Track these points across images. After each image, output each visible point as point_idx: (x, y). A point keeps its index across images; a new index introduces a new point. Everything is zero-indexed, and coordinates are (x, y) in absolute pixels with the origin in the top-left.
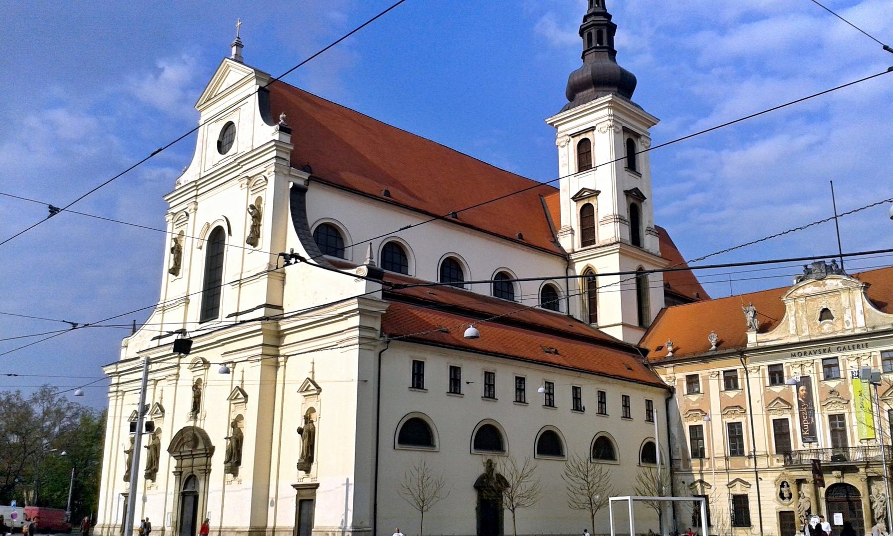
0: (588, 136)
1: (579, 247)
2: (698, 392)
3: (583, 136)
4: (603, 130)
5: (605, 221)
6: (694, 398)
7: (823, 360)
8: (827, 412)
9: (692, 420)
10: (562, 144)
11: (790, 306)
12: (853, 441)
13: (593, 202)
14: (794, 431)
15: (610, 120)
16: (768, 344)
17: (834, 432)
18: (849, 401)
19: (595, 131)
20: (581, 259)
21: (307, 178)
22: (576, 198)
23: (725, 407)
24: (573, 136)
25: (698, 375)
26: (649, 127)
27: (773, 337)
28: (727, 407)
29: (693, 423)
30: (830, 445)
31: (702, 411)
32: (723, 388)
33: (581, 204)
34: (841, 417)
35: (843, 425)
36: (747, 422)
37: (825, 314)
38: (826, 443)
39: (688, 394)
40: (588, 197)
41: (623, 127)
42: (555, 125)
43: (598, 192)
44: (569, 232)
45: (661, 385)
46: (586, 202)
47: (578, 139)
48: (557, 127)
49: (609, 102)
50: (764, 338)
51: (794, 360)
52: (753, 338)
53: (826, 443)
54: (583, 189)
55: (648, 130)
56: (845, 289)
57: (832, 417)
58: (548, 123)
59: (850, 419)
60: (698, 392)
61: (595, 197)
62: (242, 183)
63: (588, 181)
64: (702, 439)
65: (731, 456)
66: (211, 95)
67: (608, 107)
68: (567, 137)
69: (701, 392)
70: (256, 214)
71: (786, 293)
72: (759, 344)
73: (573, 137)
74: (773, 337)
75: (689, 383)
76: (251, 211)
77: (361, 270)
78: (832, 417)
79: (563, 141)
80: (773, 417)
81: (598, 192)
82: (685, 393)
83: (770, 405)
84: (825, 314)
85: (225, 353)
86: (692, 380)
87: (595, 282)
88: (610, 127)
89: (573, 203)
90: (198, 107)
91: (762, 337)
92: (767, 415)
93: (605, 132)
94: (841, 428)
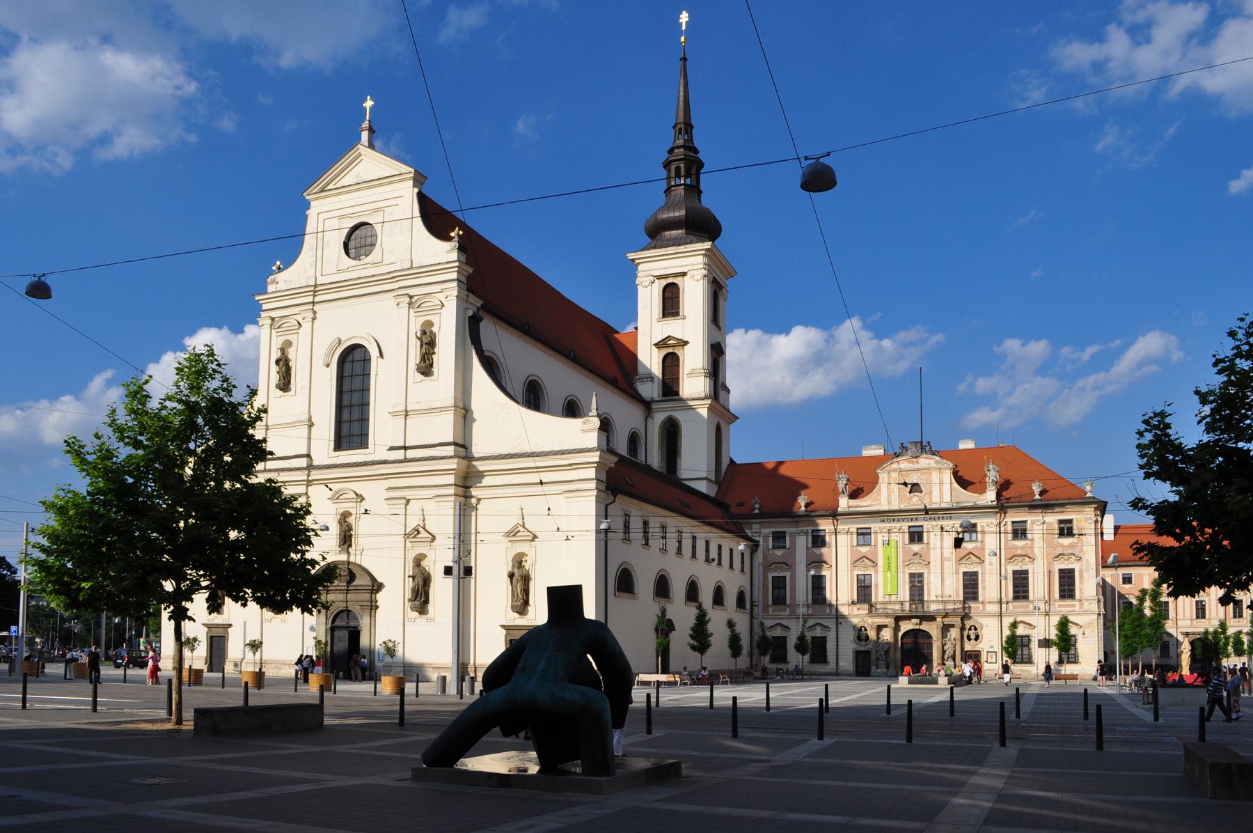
1: (659, 396)
2: (784, 547)
3: (670, 280)
4: (696, 278)
5: (692, 374)
6: (779, 553)
7: (909, 527)
8: (908, 571)
9: (776, 572)
10: (644, 284)
11: (883, 478)
12: (929, 595)
13: (678, 351)
14: (876, 585)
15: (705, 269)
16: (858, 509)
17: (912, 587)
18: (929, 563)
19: (685, 277)
20: (664, 410)
21: (480, 306)
22: (660, 345)
23: (811, 561)
24: (659, 277)
25: (785, 532)
26: (727, 279)
27: (863, 504)
28: (812, 563)
29: (776, 574)
30: (907, 598)
31: (786, 564)
32: (810, 545)
33: (665, 351)
34: (921, 575)
35: (921, 582)
36: (831, 575)
38: (904, 597)
39: (774, 548)
40: (674, 346)
41: (714, 277)
42: (637, 261)
43: (686, 343)
44: (649, 379)
46: (670, 350)
47: (664, 282)
48: (638, 264)
49: (707, 250)
50: (855, 504)
51: (882, 525)
52: (844, 503)
53: (904, 597)
54: (669, 336)
55: (727, 282)
56: (937, 468)
57: (912, 575)
58: (629, 258)
59: (929, 577)
60: (784, 547)
61: (681, 347)
62: (400, 300)
63: (672, 328)
64: (785, 588)
65: (773, 604)
66: (327, 186)
67: (704, 255)
68: (652, 278)
69: (787, 547)
70: (428, 343)
71: (882, 465)
72: (850, 509)
73: (658, 279)
74: (863, 504)
75: (774, 538)
76: (419, 335)
77: (589, 421)
78: (912, 575)
79: (646, 281)
80: (856, 572)
81: (686, 343)
82: (771, 547)
83: (856, 562)
85: (390, 488)
86: (779, 537)
87: (676, 434)
88: (705, 276)
89: (655, 350)
90: (308, 195)
91: (852, 502)
92: (852, 571)
94: (919, 585)
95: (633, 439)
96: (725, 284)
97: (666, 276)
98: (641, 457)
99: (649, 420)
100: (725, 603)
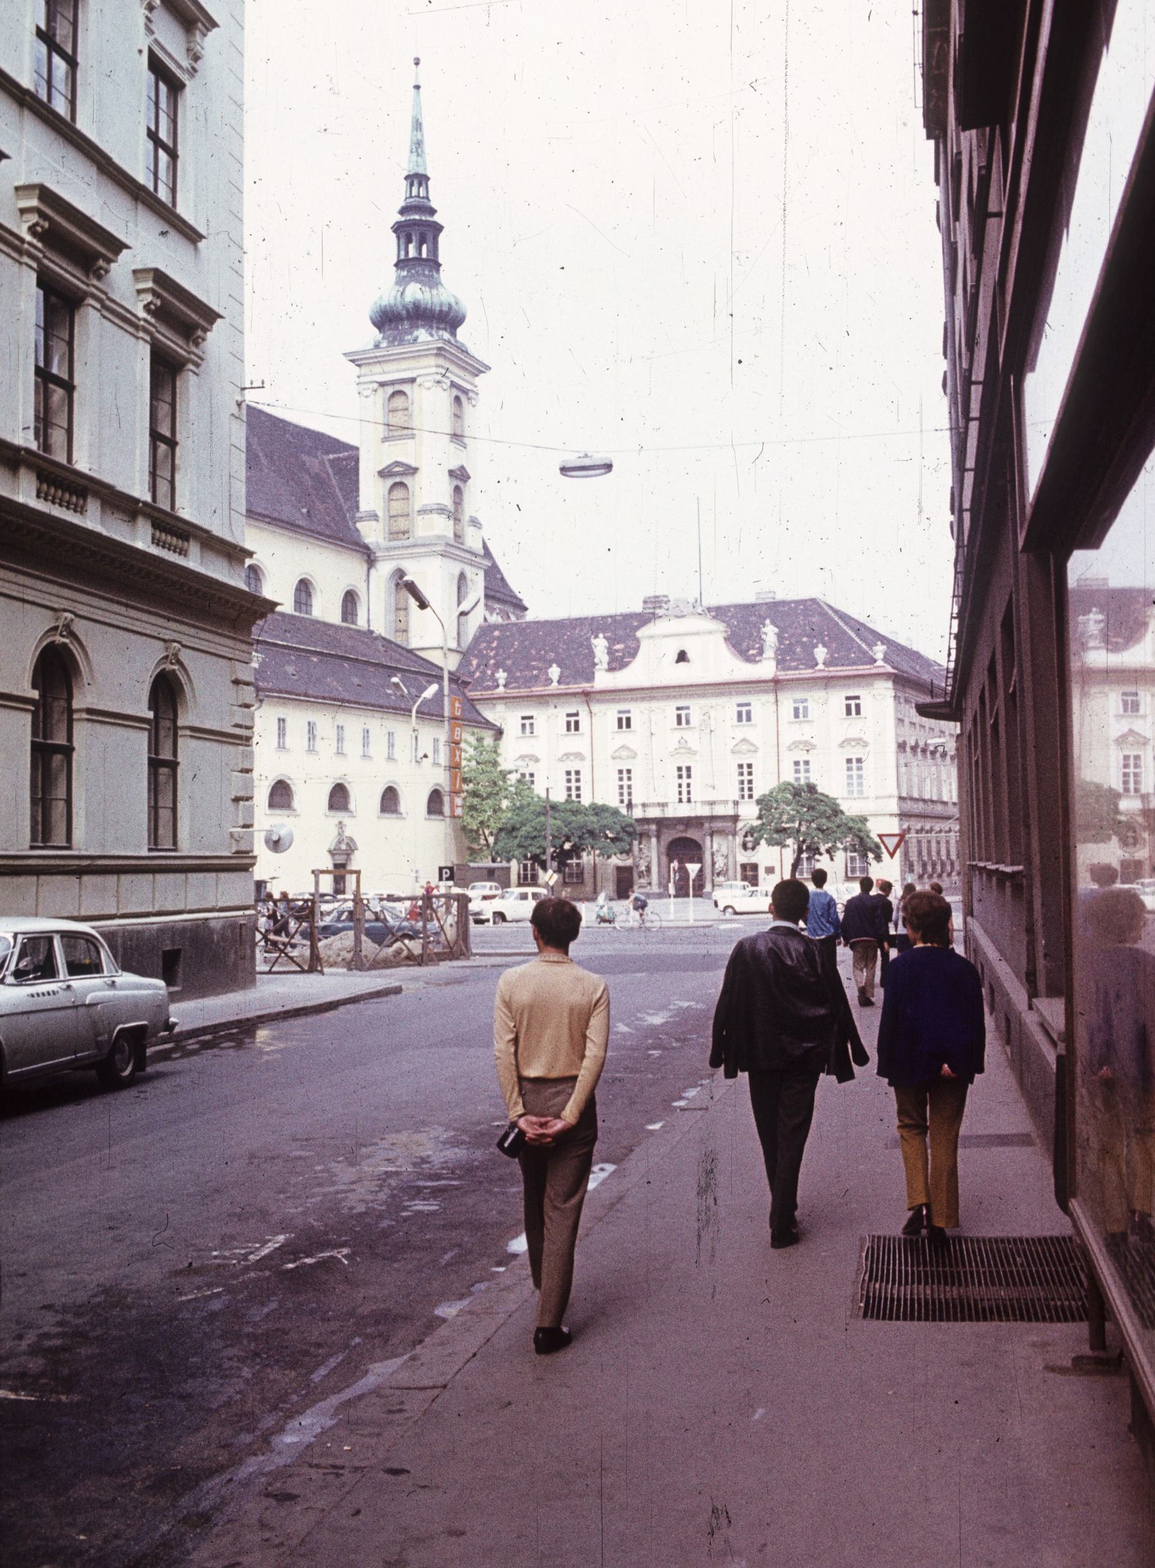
0: (405, 388)
3: (398, 387)
13: (407, 480)
19: (415, 385)
22: (383, 474)
24: (382, 384)
33: (390, 482)
37: (682, 657)
43: (415, 470)
45: (488, 725)
46: (398, 479)
47: (390, 390)
68: (375, 385)
81: (415, 470)
84: (682, 657)
93: (429, 389)
95: (350, 599)
96: (472, 384)
97: (392, 383)
98: (361, 623)
99: (373, 571)
100: (352, 806)
